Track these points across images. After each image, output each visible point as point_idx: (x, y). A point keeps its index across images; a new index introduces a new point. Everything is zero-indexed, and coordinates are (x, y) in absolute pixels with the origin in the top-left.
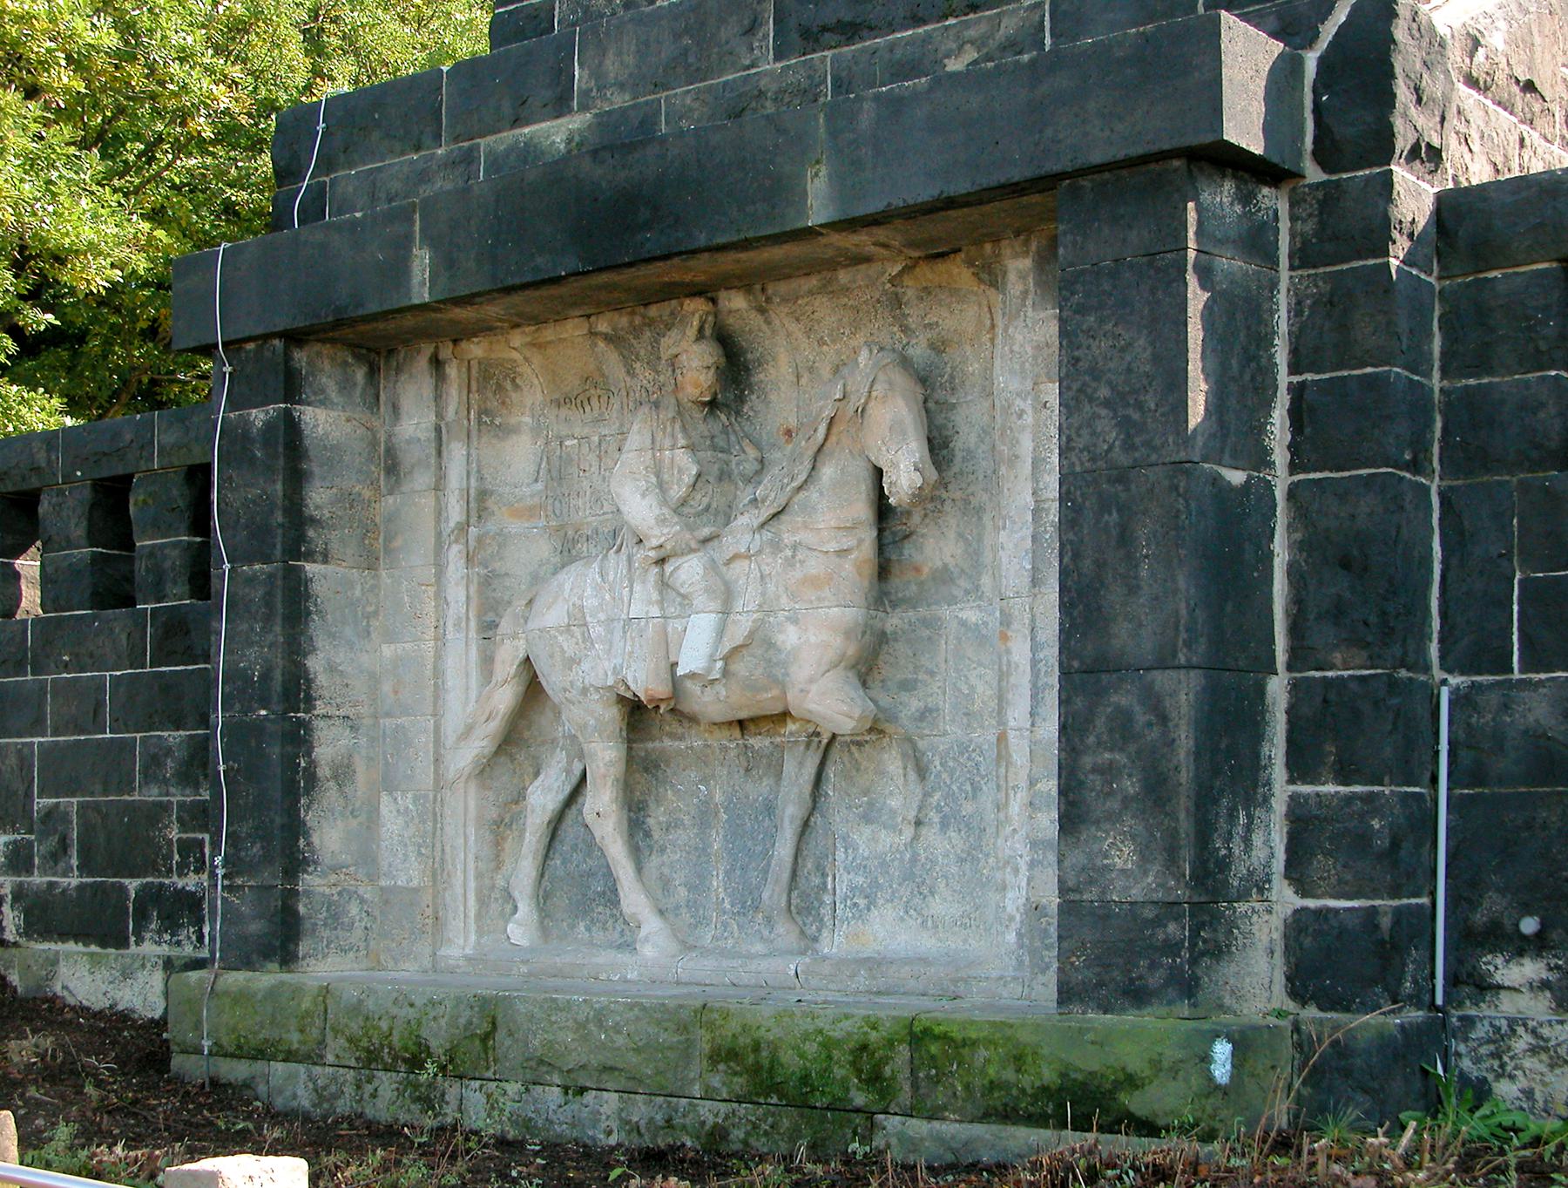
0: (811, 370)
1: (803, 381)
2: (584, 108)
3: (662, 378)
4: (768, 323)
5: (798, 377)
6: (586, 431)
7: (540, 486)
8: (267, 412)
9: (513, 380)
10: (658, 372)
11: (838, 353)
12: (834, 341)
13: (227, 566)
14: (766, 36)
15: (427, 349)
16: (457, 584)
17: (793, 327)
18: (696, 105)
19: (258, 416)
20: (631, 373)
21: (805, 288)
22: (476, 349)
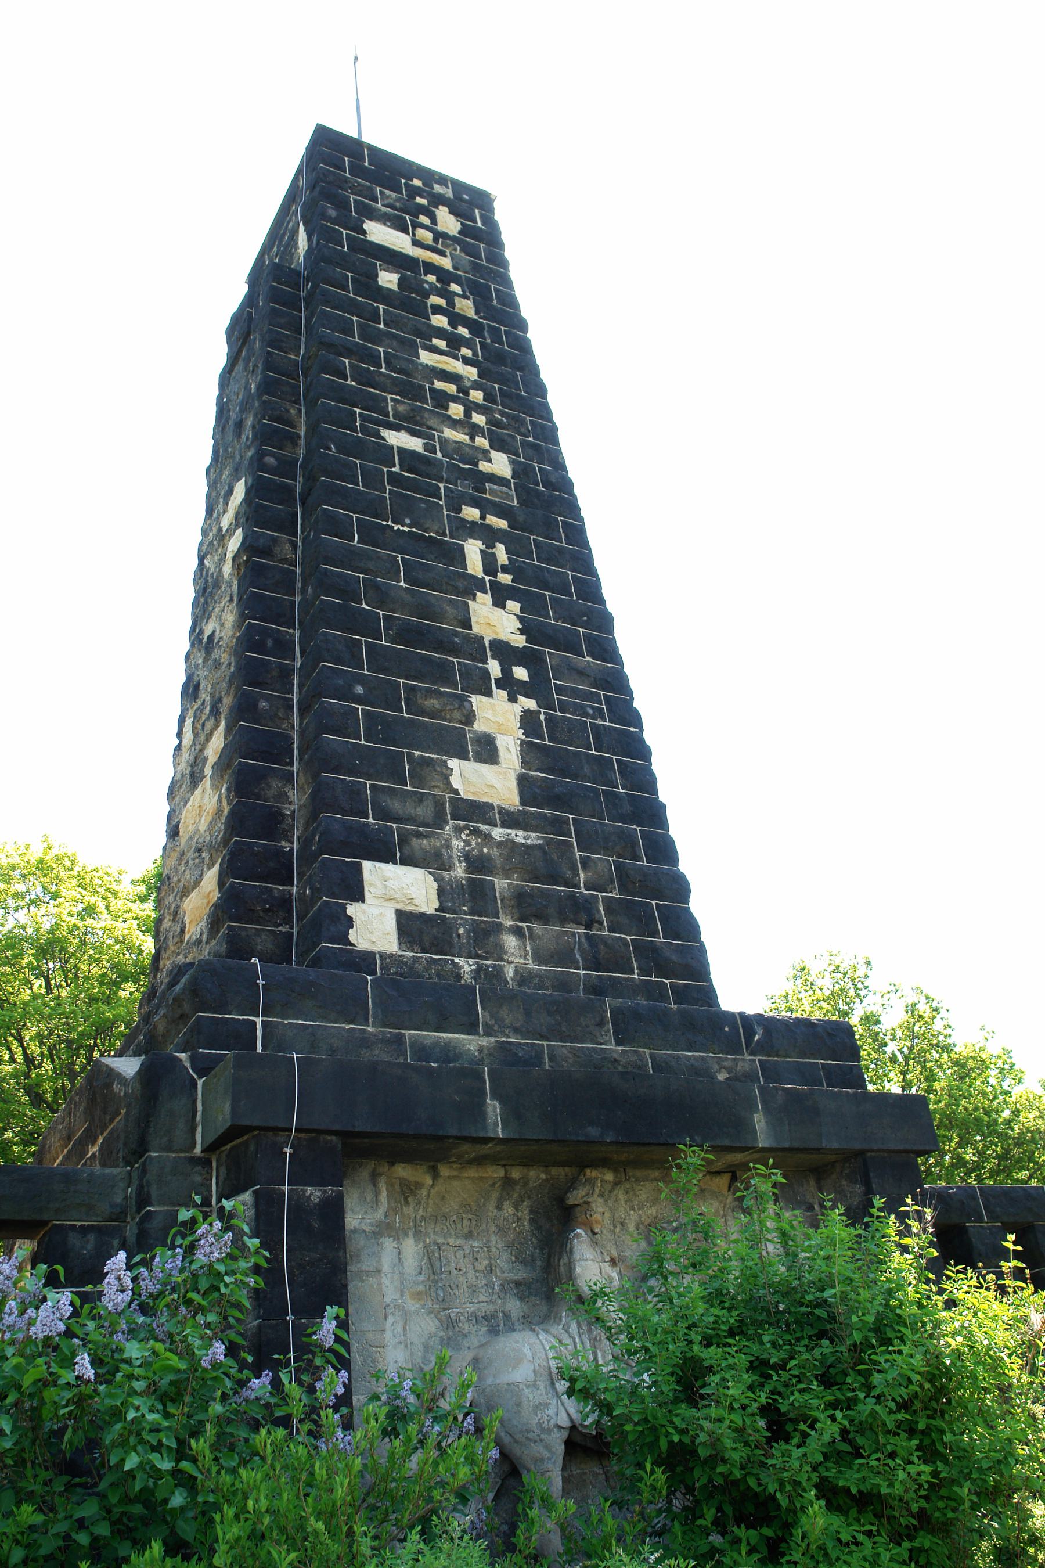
0: (622, 1224)
1: (618, 1230)
2: (488, 1034)
3: (520, 1214)
4: (610, 1192)
5: (615, 1227)
6: (459, 1242)
7: (422, 1278)
8: (325, 1192)
9: (406, 1199)
10: (517, 1210)
11: (640, 1216)
12: (639, 1209)
13: (290, 1318)
14: (609, 1030)
15: (372, 1165)
16: (395, 1348)
17: (622, 1197)
18: (570, 1055)
19: (314, 1193)
20: (499, 1207)
21: (652, 1176)
22: (402, 1171)
